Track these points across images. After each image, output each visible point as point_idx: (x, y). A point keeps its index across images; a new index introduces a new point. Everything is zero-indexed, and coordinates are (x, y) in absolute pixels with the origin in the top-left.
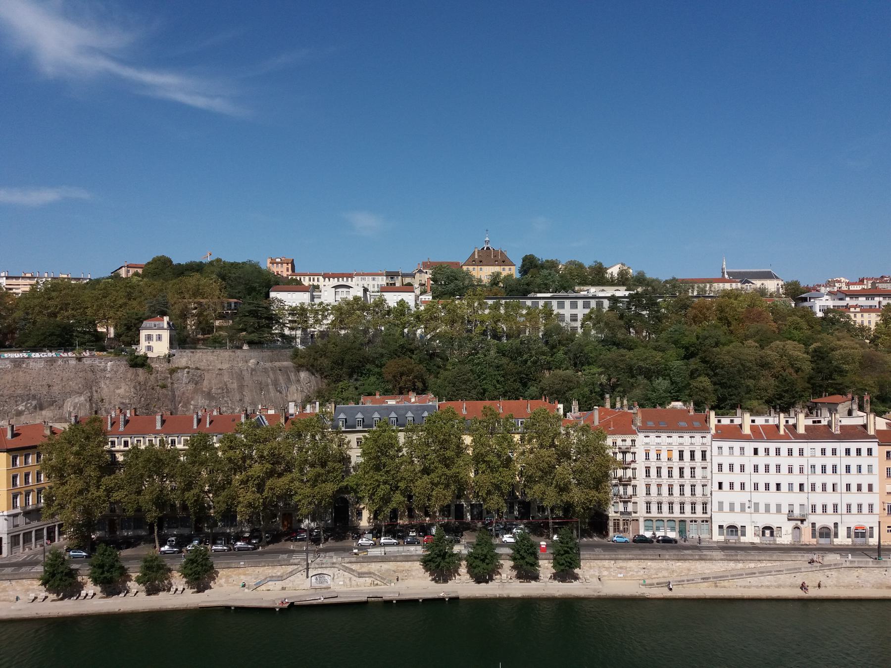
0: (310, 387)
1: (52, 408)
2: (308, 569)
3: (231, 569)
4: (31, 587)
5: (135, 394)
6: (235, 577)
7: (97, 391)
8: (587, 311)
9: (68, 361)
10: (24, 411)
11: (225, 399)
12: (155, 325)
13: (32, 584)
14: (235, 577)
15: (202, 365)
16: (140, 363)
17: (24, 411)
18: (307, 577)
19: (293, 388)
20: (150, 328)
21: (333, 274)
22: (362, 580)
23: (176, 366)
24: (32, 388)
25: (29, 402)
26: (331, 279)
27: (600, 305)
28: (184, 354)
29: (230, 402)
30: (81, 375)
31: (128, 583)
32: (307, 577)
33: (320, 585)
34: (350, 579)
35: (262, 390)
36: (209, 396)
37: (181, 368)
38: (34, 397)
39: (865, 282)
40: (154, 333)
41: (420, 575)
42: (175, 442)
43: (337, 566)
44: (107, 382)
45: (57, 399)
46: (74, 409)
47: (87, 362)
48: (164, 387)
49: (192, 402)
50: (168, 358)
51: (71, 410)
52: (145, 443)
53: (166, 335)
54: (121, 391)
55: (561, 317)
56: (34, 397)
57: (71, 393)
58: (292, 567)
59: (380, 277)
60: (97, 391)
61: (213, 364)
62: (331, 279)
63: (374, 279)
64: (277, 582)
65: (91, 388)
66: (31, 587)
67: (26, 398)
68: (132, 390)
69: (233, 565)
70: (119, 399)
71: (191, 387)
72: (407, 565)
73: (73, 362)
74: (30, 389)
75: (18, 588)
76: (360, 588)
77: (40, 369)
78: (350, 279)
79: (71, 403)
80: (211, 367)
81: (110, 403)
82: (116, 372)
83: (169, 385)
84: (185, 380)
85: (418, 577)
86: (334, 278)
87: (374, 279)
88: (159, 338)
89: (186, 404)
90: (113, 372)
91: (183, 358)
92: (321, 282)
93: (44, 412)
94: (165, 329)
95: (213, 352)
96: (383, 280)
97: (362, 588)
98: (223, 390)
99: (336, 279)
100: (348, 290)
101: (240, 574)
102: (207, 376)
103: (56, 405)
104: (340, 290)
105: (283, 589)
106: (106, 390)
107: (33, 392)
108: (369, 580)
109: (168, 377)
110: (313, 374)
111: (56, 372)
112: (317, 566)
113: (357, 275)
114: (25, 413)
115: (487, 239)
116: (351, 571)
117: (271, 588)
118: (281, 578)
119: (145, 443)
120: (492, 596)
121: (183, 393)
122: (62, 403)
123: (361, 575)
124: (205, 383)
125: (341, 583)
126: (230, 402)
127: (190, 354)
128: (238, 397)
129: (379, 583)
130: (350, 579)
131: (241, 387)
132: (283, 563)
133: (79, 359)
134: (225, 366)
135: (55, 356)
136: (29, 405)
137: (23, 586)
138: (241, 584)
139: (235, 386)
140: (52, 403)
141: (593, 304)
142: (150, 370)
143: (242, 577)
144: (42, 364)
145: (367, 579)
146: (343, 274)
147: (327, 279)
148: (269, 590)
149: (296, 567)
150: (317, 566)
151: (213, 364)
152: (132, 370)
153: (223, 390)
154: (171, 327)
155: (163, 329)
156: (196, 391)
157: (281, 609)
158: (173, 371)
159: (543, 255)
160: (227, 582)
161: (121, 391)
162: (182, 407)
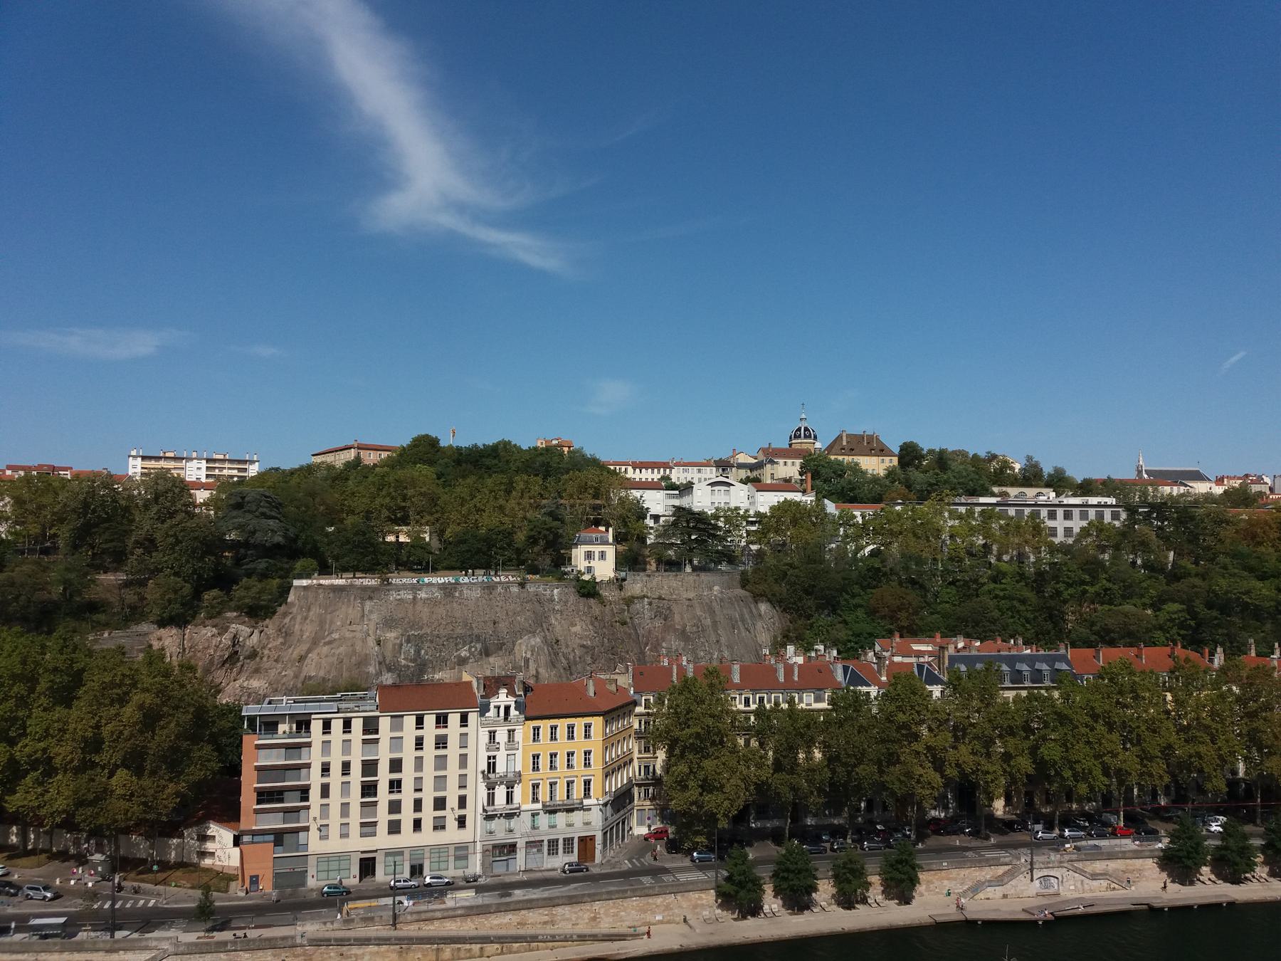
0: (774, 624)
1: (501, 653)
2: (1032, 870)
3: (932, 872)
4: (699, 902)
5: (595, 633)
6: (937, 883)
7: (548, 630)
8: (1084, 523)
9: (508, 587)
10: (469, 658)
11: (702, 640)
12: (597, 539)
13: (700, 898)
14: (937, 883)
15: (664, 592)
16: (588, 590)
17: (469, 658)
18: (1032, 880)
19: (759, 625)
20: (590, 543)
21: (642, 463)
22: (1096, 883)
23: (629, 594)
24: (474, 626)
25: (472, 645)
26: (643, 470)
27: (1100, 516)
28: (638, 578)
29: (707, 644)
30: (528, 606)
31: (814, 895)
32: (1032, 880)
33: (1047, 890)
34: (1082, 881)
35: (734, 628)
36: (684, 635)
37: (637, 598)
38: (478, 638)
39: (1225, 482)
40: (596, 549)
41: (1155, 876)
42: (763, 700)
43: (1066, 865)
44: (558, 616)
45: (505, 641)
46: (532, 655)
47: (531, 588)
48: (624, 623)
49: (664, 645)
50: (619, 583)
51: (529, 656)
52: (769, 701)
53: (610, 552)
54: (577, 629)
55: (1053, 532)
56: (478, 638)
57: (520, 633)
58: (1002, 867)
59: (708, 468)
60: (548, 630)
61: (676, 592)
62: (643, 470)
63: (699, 471)
64: (997, 888)
65: (542, 626)
66: (699, 902)
67: (468, 640)
68: (591, 627)
69: (934, 867)
70: (578, 641)
71: (658, 623)
72: (1138, 863)
73: (515, 589)
74: (471, 628)
75: (685, 905)
76: (1094, 894)
77: (477, 599)
78: (656, 470)
79: (527, 646)
80: (674, 597)
81: (567, 646)
82: (566, 602)
83: (628, 620)
84: (647, 614)
85: (1153, 879)
86: (647, 469)
87: (699, 471)
88: (603, 556)
89: (656, 648)
90: (562, 604)
91: (637, 585)
92: (692, 474)
93: (491, 659)
94: (611, 544)
95: (677, 575)
96: (711, 473)
97: (1098, 894)
98: (698, 627)
99: (650, 470)
100: (727, 488)
101: (943, 879)
102: (675, 608)
103: (506, 650)
104: (716, 488)
105: (1005, 896)
106: (558, 628)
107: (476, 631)
108: (1104, 883)
109: (624, 610)
110: (774, 607)
111: (497, 604)
112: (1043, 866)
113: (678, 464)
114: (471, 661)
115: (803, 416)
116: (1082, 872)
117: (990, 895)
118: (999, 881)
119: (754, 702)
120: (1272, 899)
121: (650, 632)
122: (511, 646)
123: (1094, 876)
124: (677, 617)
125: (1072, 887)
126: (707, 644)
127: (645, 578)
128: (713, 638)
129: (1116, 886)
130: (1082, 881)
131: (715, 623)
132: (992, 862)
133: (522, 585)
134: (691, 595)
135: (486, 580)
136: (473, 649)
137: (690, 901)
138: (946, 892)
139: (708, 622)
140: (500, 647)
141: (1092, 513)
142: (602, 602)
143: (946, 882)
144: (477, 593)
145: (1102, 881)
146: (655, 463)
147: (638, 470)
148: (988, 899)
149: (1007, 868)
150: (1043, 866)
151: (676, 592)
152: (583, 600)
153: (698, 627)
154: (618, 539)
155: (607, 543)
156: (667, 628)
157: (1045, 922)
158: (629, 601)
159: (928, 442)
160: (928, 889)
161: (577, 629)
162: (651, 650)
